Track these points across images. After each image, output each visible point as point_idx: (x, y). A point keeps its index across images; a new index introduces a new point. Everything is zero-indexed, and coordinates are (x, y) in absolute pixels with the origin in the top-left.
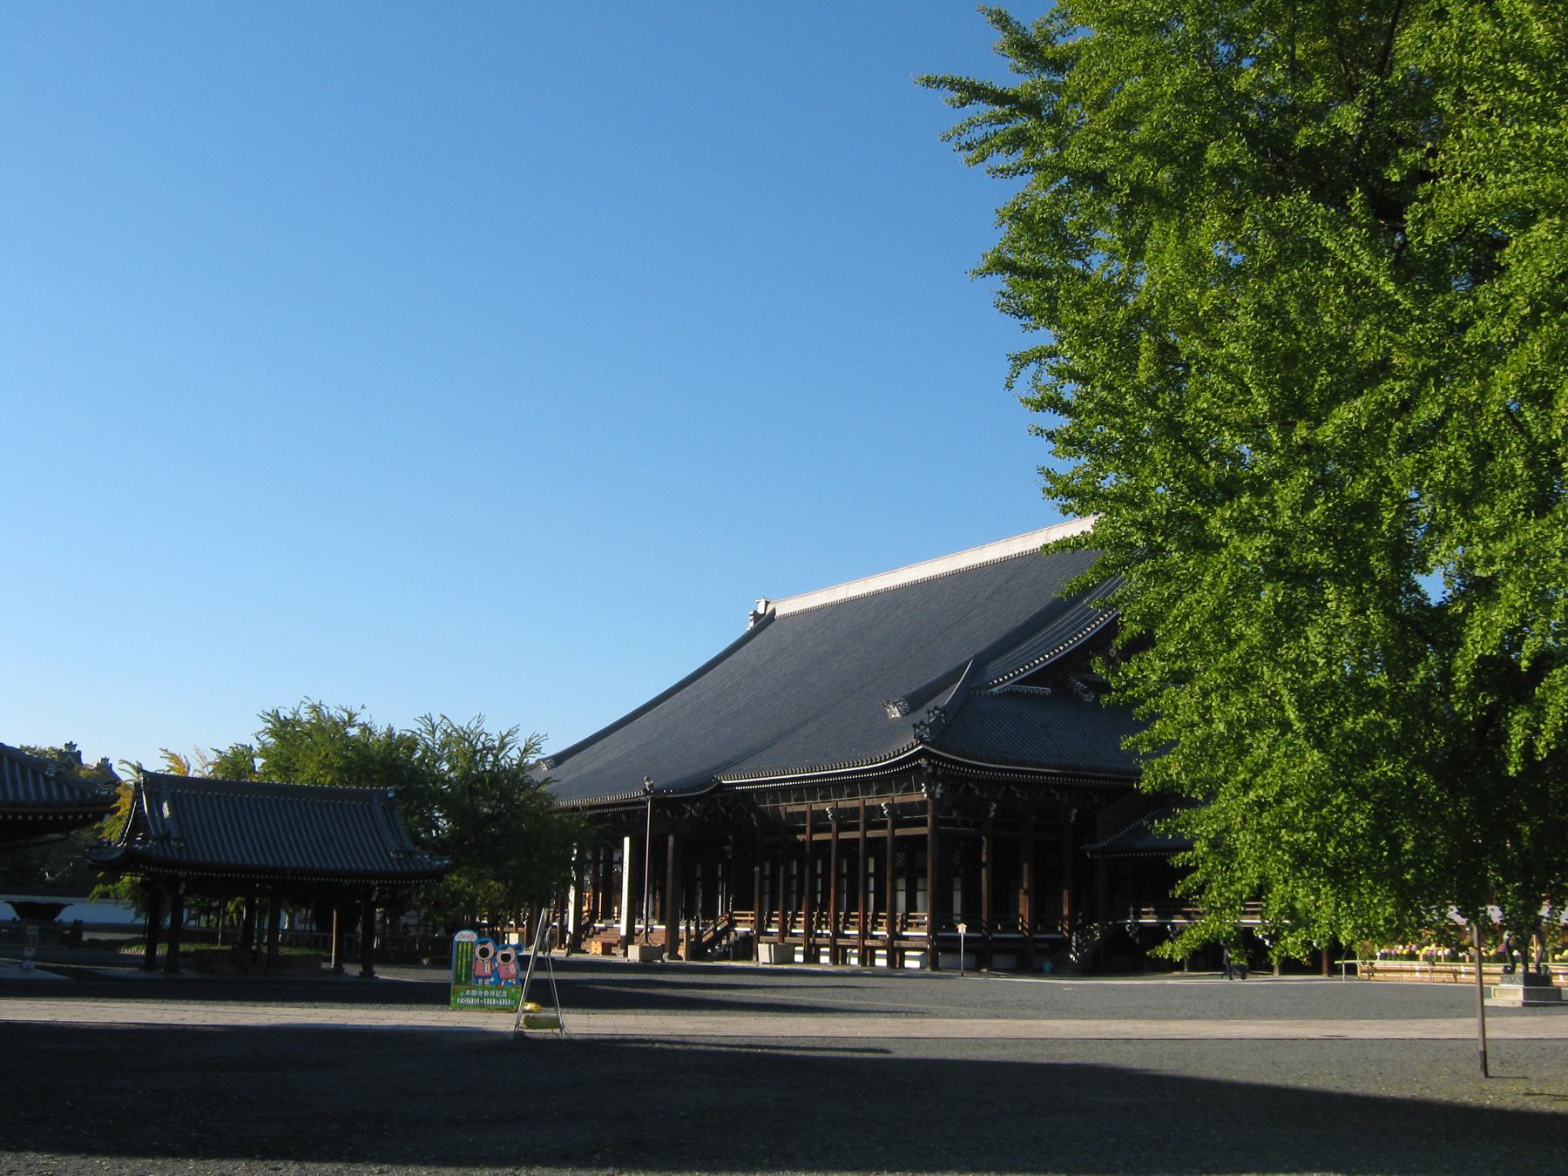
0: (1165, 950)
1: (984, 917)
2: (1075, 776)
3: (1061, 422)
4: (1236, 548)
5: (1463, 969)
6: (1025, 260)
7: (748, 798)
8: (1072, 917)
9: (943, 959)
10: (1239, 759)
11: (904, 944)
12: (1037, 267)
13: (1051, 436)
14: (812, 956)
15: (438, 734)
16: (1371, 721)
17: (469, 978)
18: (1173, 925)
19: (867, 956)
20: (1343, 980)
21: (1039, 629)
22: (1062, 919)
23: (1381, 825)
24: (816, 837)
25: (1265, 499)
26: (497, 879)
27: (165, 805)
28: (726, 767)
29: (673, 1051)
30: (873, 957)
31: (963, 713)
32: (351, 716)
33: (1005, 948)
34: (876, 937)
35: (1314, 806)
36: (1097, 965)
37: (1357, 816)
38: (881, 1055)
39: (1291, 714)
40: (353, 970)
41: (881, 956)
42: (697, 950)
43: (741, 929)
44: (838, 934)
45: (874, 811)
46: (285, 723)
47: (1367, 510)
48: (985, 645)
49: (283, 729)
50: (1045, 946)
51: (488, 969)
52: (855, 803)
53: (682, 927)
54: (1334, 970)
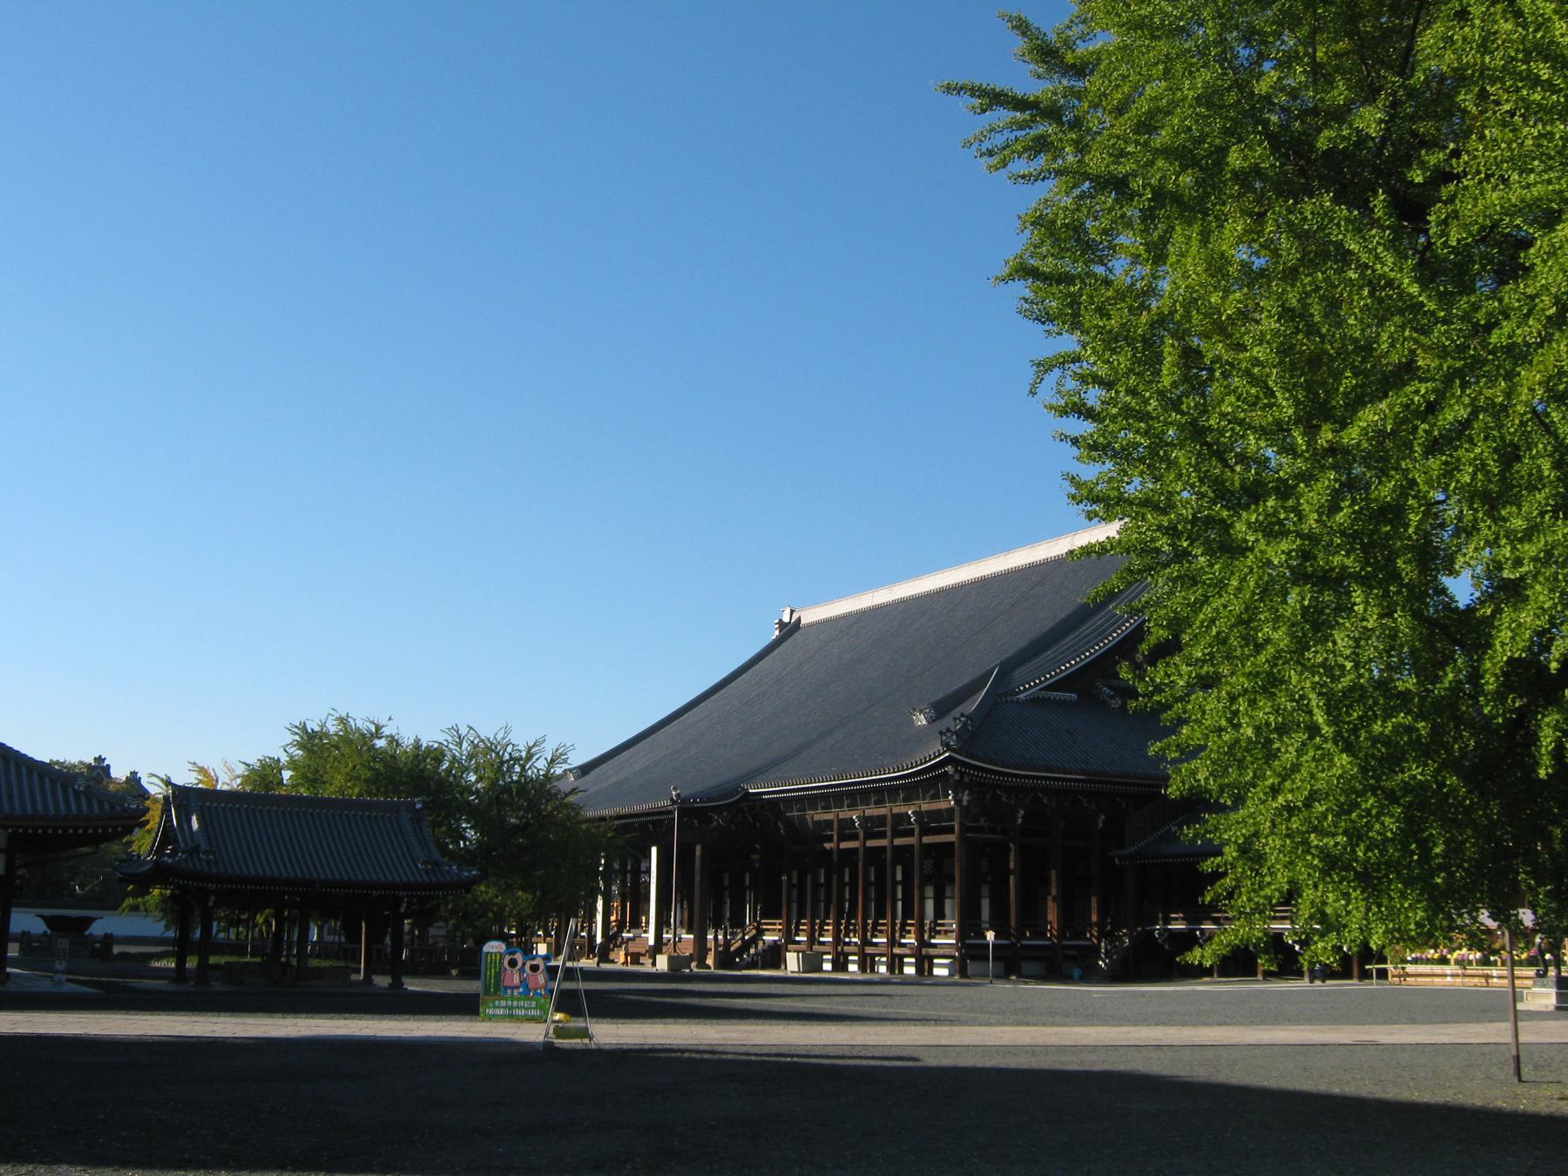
0: (1195, 956)
1: (1013, 924)
2: (1100, 782)
3: (1085, 428)
4: (1262, 552)
5: (1495, 973)
6: (1047, 266)
7: (774, 806)
8: (1101, 924)
9: (972, 967)
10: (1269, 763)
11: (932, 951)
12: (1059, 272)
13: (1075, 441)
14: (840, 965)
15: (465, 745)
16: (1400, 724)
17: (498, 988)
18: (1202, 931)
19: (895, 963)
20: (1374, 985)
22: (1091, 925)
23: (1412, 829)
24: (843, 845)
25: (1290, 503)
26: (523, 890)
27: (194, 818)
28: (752, 776)
29: (702, 1060)
30: (902, 965)
31: (989, 721)
32: (378, 728)
33: (1031, 954)
34: (904, 945)
35: (1344, 810)
36: (1126, 972)
37: (1387, 820)
38: (910, 1064)
39: (1320, 718)
40: (383, 981)
41: (910, 964)
42: (725, 960)
43: (768, 938)
44: (866, 942)
46: (312, 735)
47: (1394, 513)
49: (311, 741)
50: (1072, 952)
53: (710, 937)
54: (1365, 975)
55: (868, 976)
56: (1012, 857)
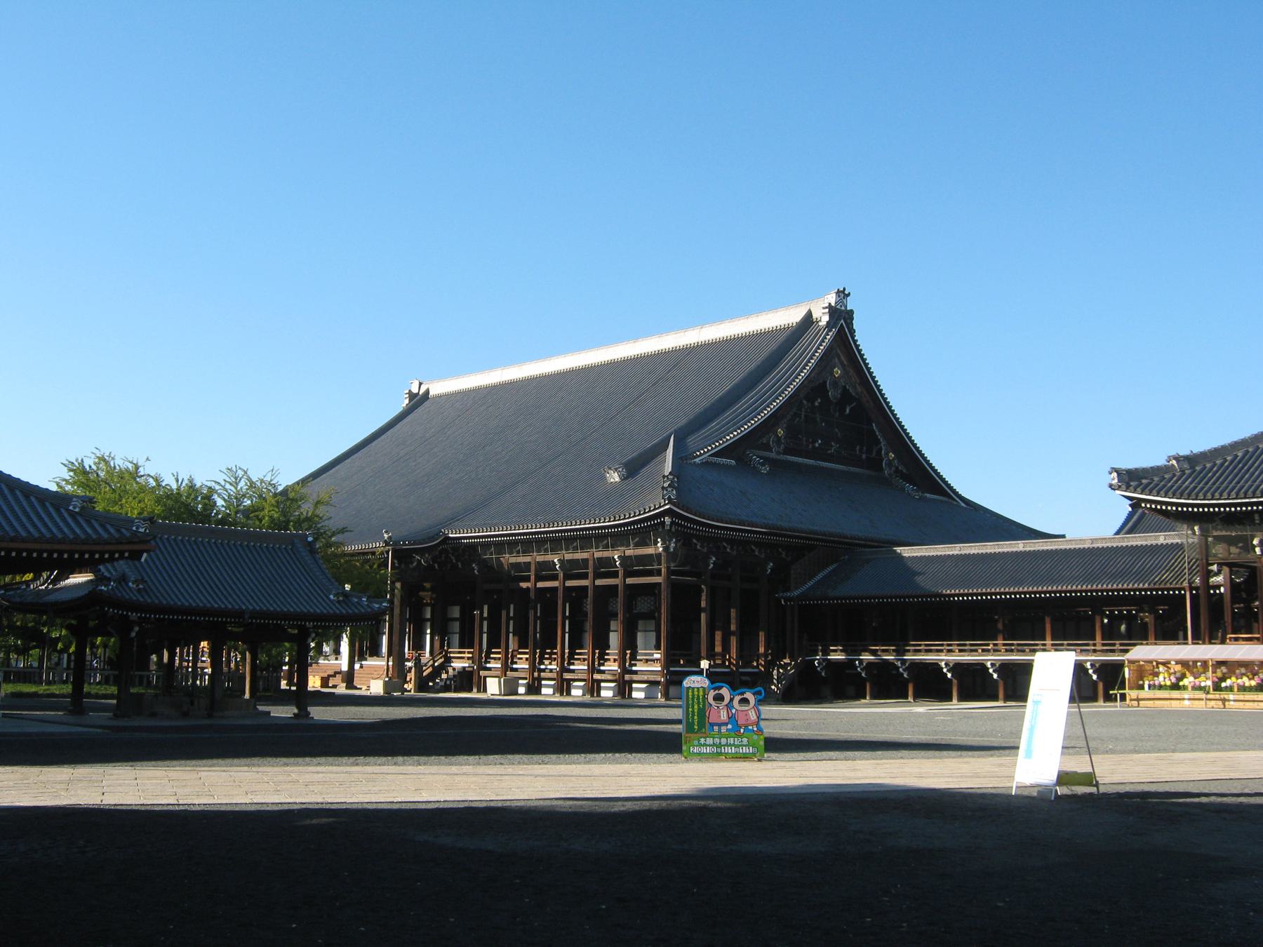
7: (470, 551)
9: (672, 690)
11: (635, 677)
14: (534, 688)
15: (242, 484)
18: (861, 661)
20: (1117, 706)
21: (724, 410)
24: (540, 585)
28: (451, 521)
32: (137, 467)
34: (603, 672)
42: (422, 685)
43: (457, 665)
45: (609, 562)
48: (683, 422)
51: (724, 716)
52: (585, 555)
55: (557, 698)
56: (704, 597)
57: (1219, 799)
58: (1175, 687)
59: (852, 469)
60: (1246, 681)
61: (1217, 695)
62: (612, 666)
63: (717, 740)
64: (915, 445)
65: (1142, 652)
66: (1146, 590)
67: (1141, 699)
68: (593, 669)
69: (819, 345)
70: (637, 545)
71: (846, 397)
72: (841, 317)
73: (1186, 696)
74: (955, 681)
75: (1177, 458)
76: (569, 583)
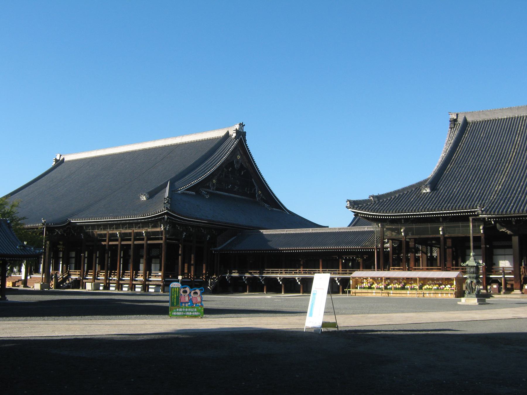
2: (213, 224)
5: (391, 292)
7: (81, 228)
9: (166, 288)
11: (150, 283)
14: (107, 287)
18: (245, 277)
20: (347, 296)
24: (110, 243)
28: (72, 215)
30: (135, 288)
34: (137, 281)
42: (57, 286)
43: (73, 277)
48: (173, 176)
50: (198, 284)
51: (187, 299)
52: (130, 231)
55: (117, 292)
56: (180, 249)
57: (385, 333)
58: (370, 288)
59: (243, 197)
60: (397, 286)
61: (386, 291)
62: (141, 278)
63: (184, 310)
64: (269, 188)
65: (357, 274)
66: (359, 249)
67: (357, 293)
68: (132, 279)
69: (231, 146)
70: (153, 227)
71: (242, 167)
72: (241, 134)
73: (374, 292)
74: (283, 285)
75: (373, 196)
76: (123, 243)
